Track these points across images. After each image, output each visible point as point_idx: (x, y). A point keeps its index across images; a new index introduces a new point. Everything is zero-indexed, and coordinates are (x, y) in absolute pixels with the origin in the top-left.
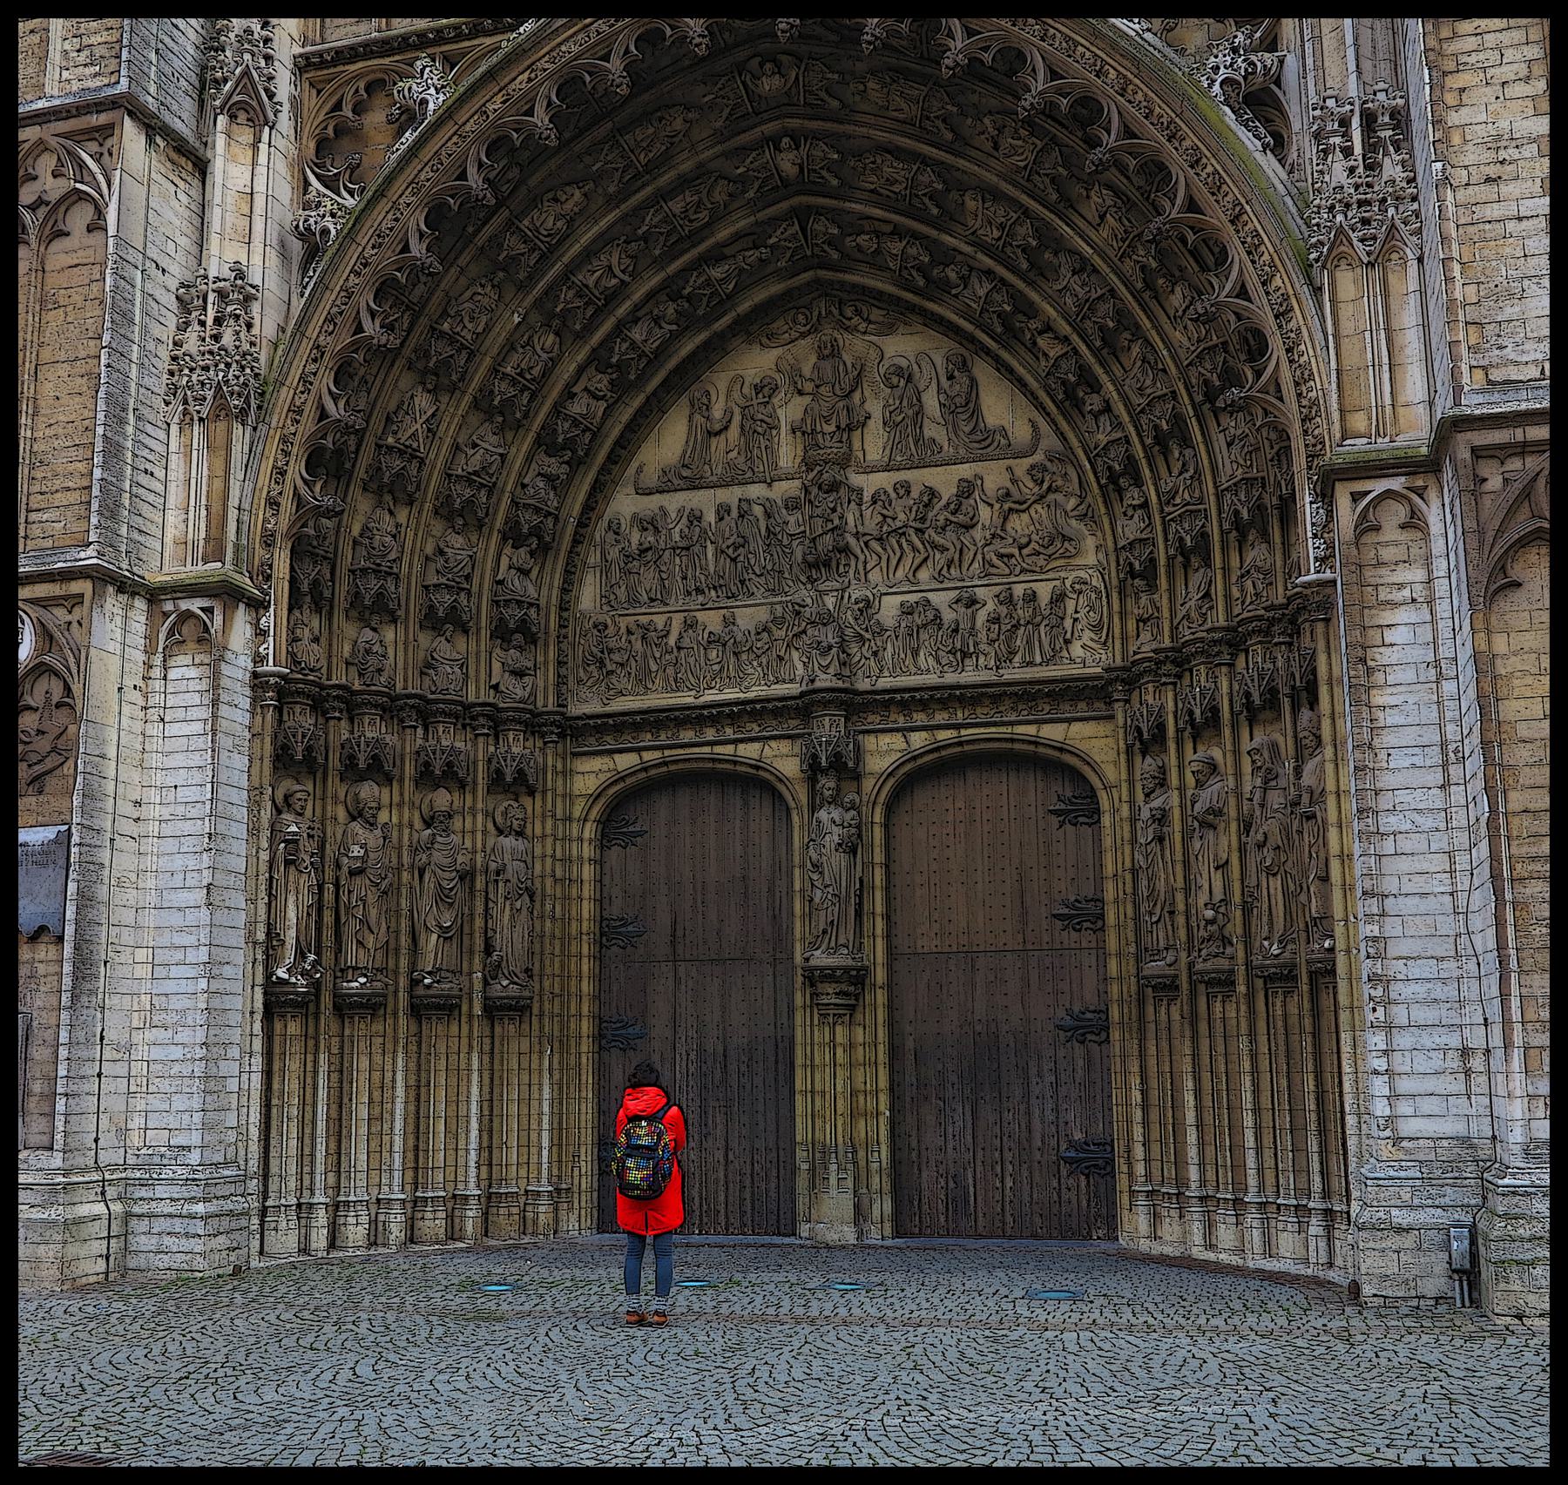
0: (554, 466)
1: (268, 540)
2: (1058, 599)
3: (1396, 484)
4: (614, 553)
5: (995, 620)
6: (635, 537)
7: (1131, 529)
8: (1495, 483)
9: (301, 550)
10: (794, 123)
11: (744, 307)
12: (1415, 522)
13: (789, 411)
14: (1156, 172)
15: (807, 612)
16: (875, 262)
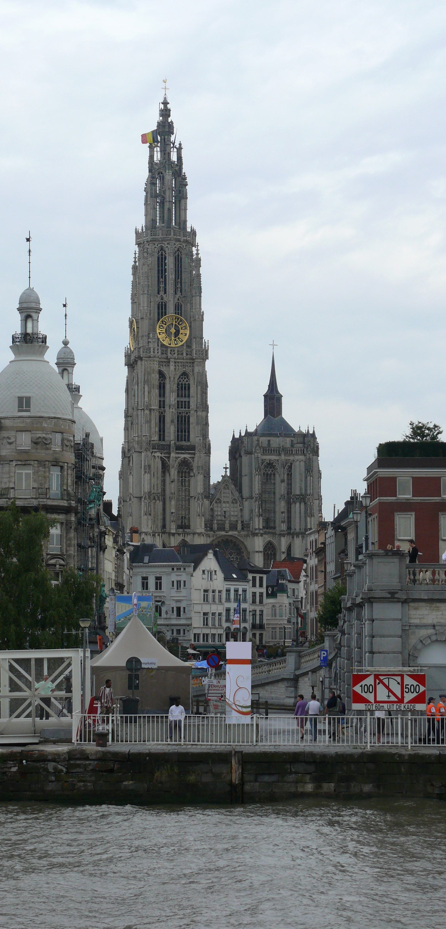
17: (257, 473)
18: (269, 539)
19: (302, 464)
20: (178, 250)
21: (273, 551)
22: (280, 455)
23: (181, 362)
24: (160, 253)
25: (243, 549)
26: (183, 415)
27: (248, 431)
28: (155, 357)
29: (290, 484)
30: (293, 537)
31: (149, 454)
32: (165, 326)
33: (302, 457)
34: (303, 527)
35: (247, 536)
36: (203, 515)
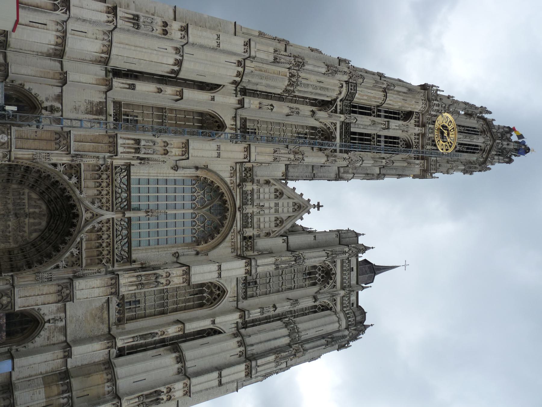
0: (30, 185)
1: (17, 162)
2: (9, 242)
3: (11, 282)
4: (19, 190)
5: (7, 235)
6: (22, 192)
7: (16, 252)
8: (8, 291)
9: (16, 165)
10: (68, 217)
11: (50, 207)
12: (7, 284)
13: (37, 210)
14: (51, 258)
15: (9, 214)
16: (53, 223)
17: (330, 253)
18: (229, 290)
19: (336, 326)
20: (481, 150)
21: (208, 300)
22: (343, 288)
23: (418, 143)
24: (479, 130)
25: (211, 242)
26: (372, 143)
27: (360, 238)
28: (430, 106)
29: (304, 312)
30: (235, 335)
31: (346, 78)
32: (447, 125)
33: (344, 325)
34: (256, 349)
35: (234, 249)
36: (275, 159)
